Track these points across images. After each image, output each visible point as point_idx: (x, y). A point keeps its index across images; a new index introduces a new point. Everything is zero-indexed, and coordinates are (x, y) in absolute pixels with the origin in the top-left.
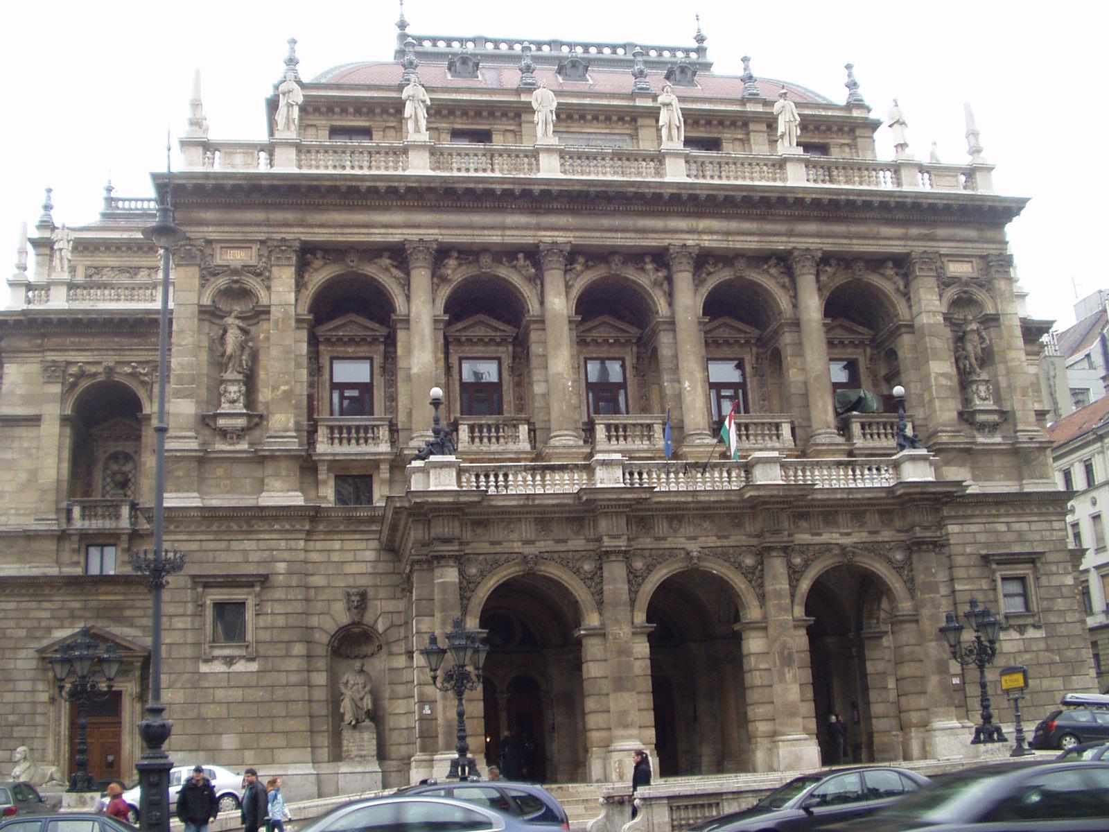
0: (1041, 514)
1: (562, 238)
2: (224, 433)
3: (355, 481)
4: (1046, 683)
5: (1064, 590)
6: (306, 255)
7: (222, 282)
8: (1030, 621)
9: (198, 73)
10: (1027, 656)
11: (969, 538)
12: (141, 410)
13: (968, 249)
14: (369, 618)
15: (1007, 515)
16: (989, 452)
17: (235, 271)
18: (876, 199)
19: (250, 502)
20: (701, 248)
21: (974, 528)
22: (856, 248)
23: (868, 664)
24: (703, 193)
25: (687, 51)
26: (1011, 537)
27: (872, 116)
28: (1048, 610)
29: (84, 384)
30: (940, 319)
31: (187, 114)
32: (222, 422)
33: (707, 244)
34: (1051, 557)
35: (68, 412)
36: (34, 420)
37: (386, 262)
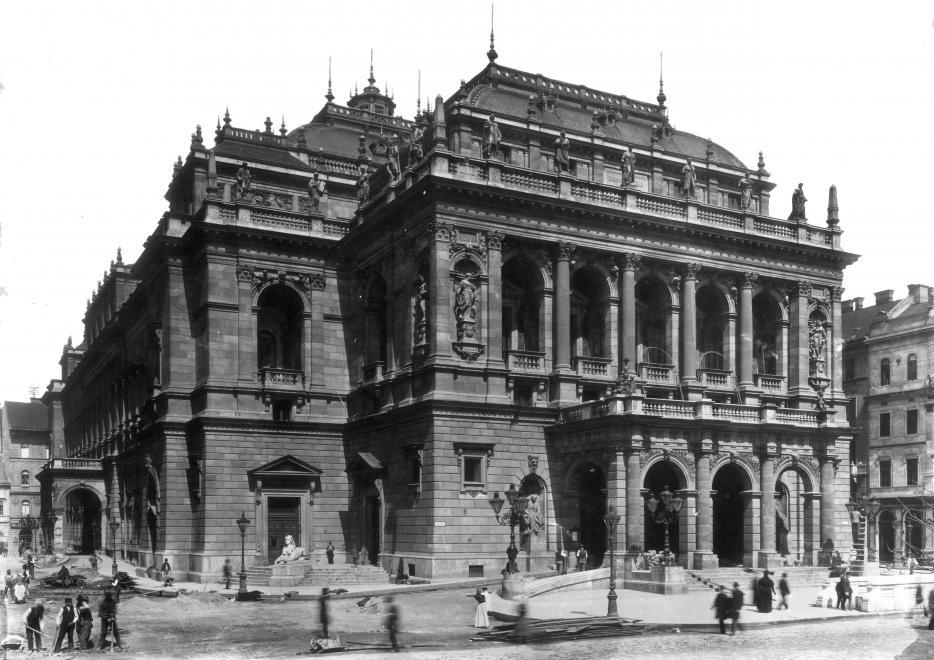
1: (638, 251)
2: (464, 356)
3: (523, 387)
7: (460, 256)
12: (303, 308)
14: (538, 472)
17: (468, 250)
19: (479, 398)
20: (703, 268)
27: (769, 180)
29: (265, 286)
32: (465, 349)
33: (704, 264)
35: (255, 305)
36: (235, 308)
37: (544, 252)
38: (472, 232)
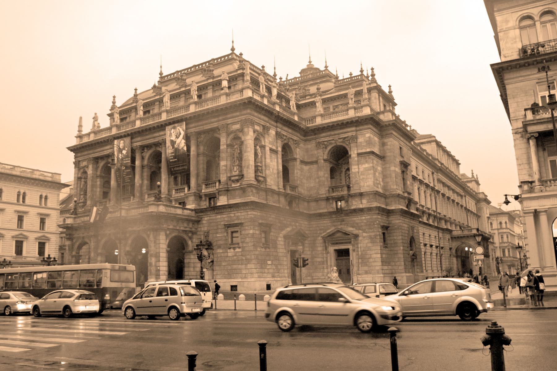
0: (244, 210)
4: (240, 266)
5: (249, 235)
6: (97, 160)
8: (237, 246)
9: (81, 118)
10: (235, 257)
11: (223, 219)
13: (237, 119)
15: (234, 211)
16: (235, 189)
18: (205, 112)
21: (224, 216)
22: (205, 128)
23: (185, 260)
24: (156, 125)
25: (228, 55)
26: (235, 218)
28: (242, 242)
30: (225, 146)
31: (77, 129)
34: (246, 224)
38: (84, 160)
